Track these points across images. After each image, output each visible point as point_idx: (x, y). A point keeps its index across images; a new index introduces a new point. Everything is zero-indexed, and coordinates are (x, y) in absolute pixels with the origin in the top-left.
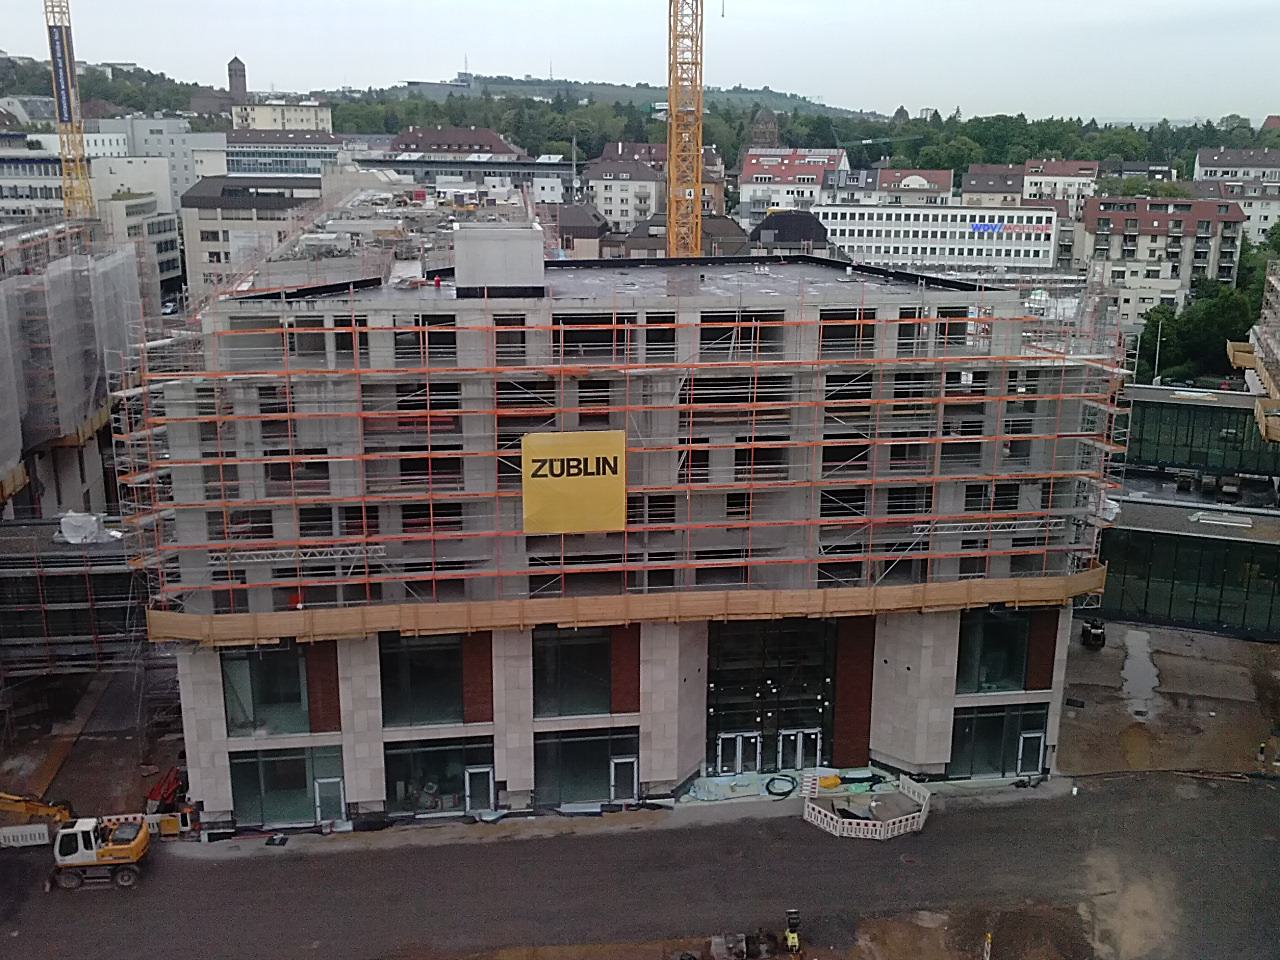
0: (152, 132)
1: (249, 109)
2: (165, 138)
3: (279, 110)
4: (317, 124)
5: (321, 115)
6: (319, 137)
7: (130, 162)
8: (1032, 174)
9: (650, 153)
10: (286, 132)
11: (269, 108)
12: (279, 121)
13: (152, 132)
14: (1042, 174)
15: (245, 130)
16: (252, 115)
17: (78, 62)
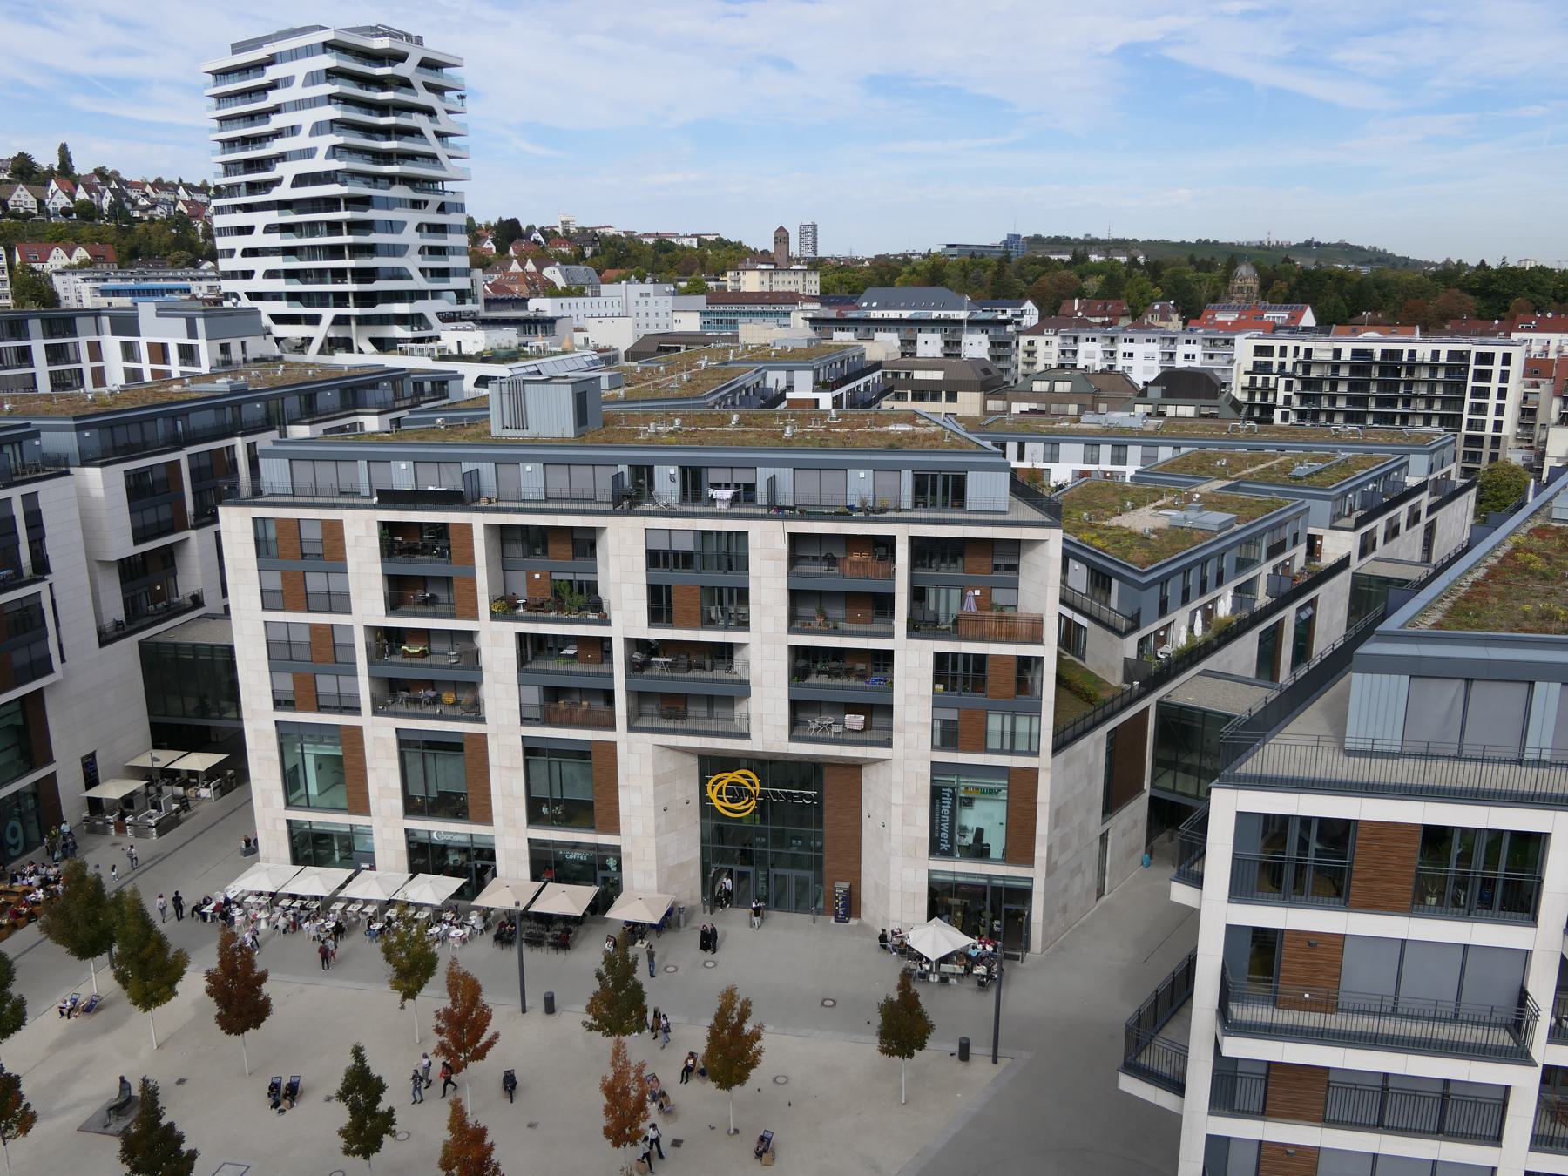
0: (642, 295)
1: (741, 273)
2: (652, 299)
3: (767, 274)
4: (771, 286)
5: (808, 278)
6: (792, 298)
7: (600, 322)
8: (1522, 330)
9: (1105, 309)
10: (771, 293)
11: (757, 272)
12: (767, 283)
13: (642, 295)
14: (1536, 330)
15: (737, 292)
16: (743, 278)
17: (219, 229)
